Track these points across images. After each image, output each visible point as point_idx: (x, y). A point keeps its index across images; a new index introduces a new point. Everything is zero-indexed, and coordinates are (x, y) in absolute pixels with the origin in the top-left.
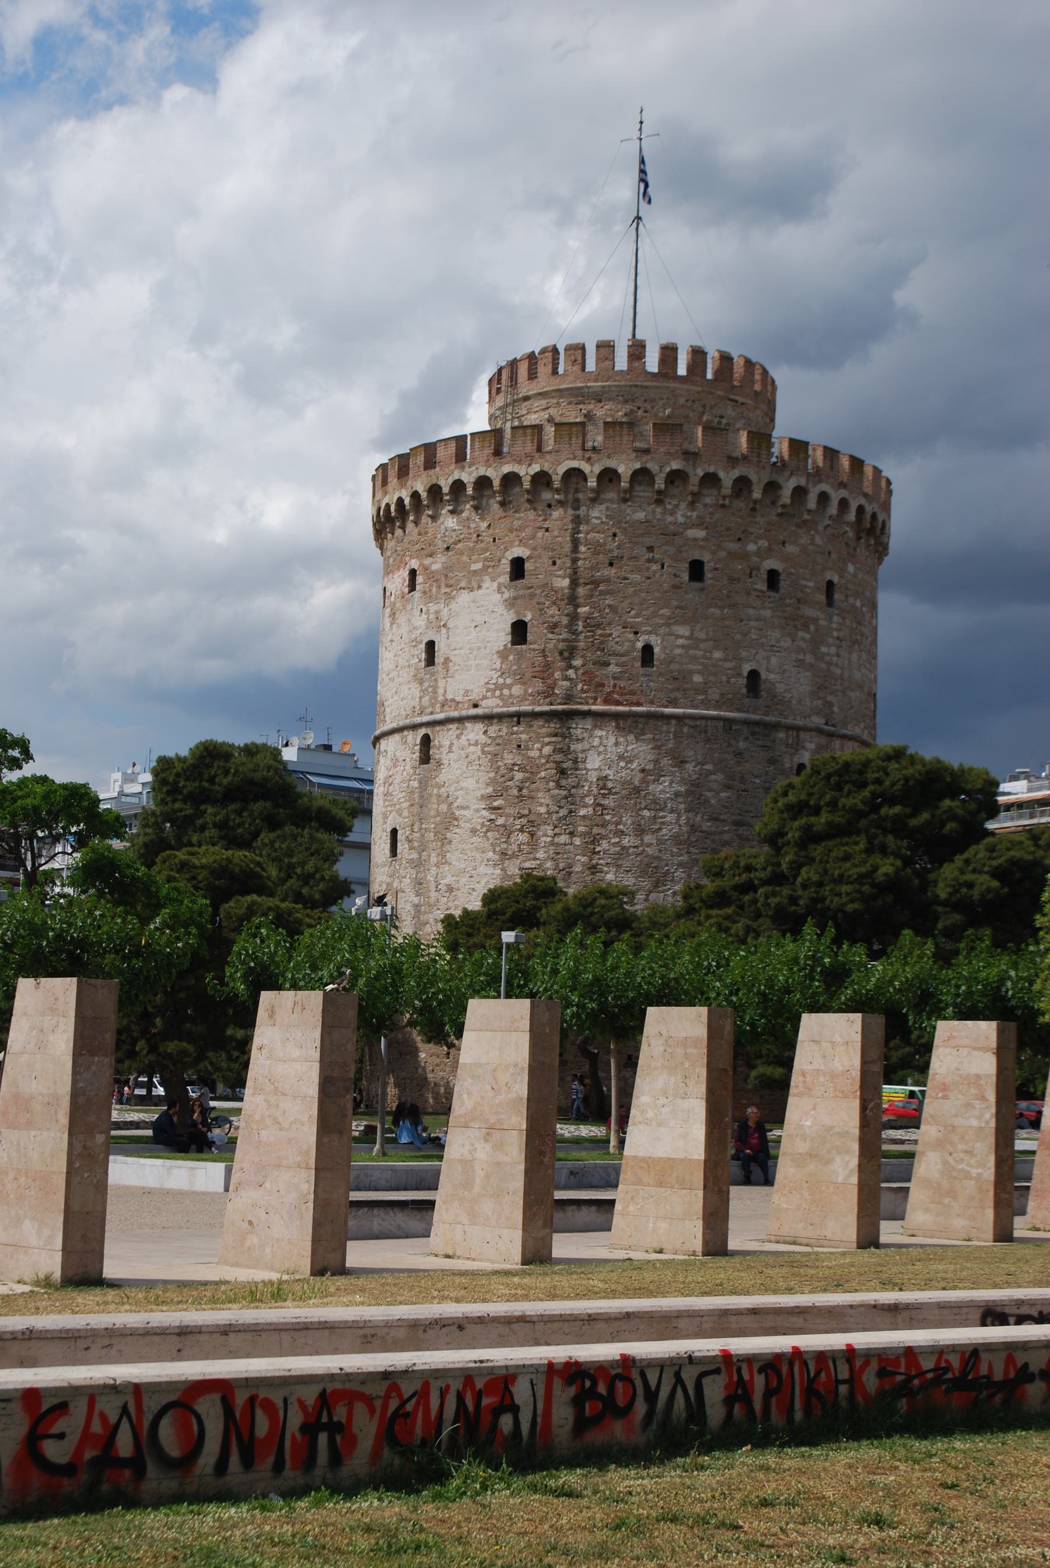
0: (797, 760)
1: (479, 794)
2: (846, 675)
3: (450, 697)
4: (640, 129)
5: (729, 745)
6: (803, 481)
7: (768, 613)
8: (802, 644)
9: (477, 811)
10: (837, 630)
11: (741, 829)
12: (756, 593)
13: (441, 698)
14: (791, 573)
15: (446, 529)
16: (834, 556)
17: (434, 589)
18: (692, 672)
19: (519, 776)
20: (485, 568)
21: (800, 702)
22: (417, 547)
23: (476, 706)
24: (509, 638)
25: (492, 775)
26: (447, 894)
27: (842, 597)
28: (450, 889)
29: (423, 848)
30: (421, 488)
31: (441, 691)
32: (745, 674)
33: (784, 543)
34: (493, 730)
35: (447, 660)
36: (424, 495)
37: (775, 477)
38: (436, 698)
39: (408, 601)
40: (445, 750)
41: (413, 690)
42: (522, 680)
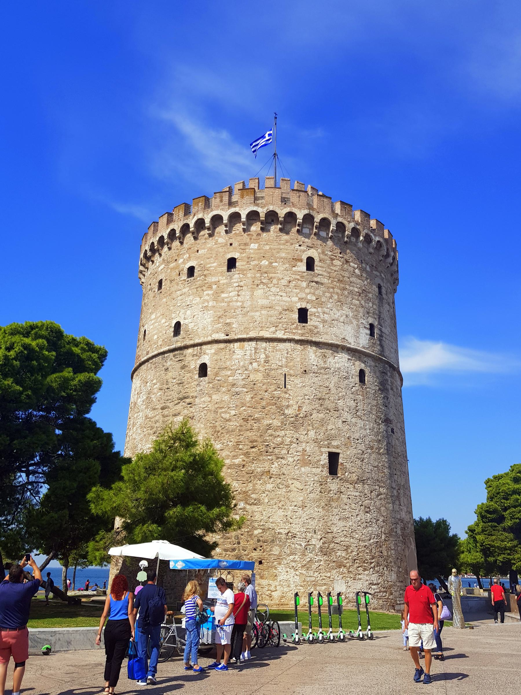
0: (199, 362)
2: (248, 304)
5: (163, 366)
6: (200, 216)
7: (188, 289)
8: (207, 298)
10: (236, 282)
11: (164, 411)
12: (181, 282)
14: (201, 264)
16: (235, 244)
18: (154, 335)
21: (204, 329)
27: (245, 263)
32: (173, 326)
33: (198, 251)
37: (185, 222)
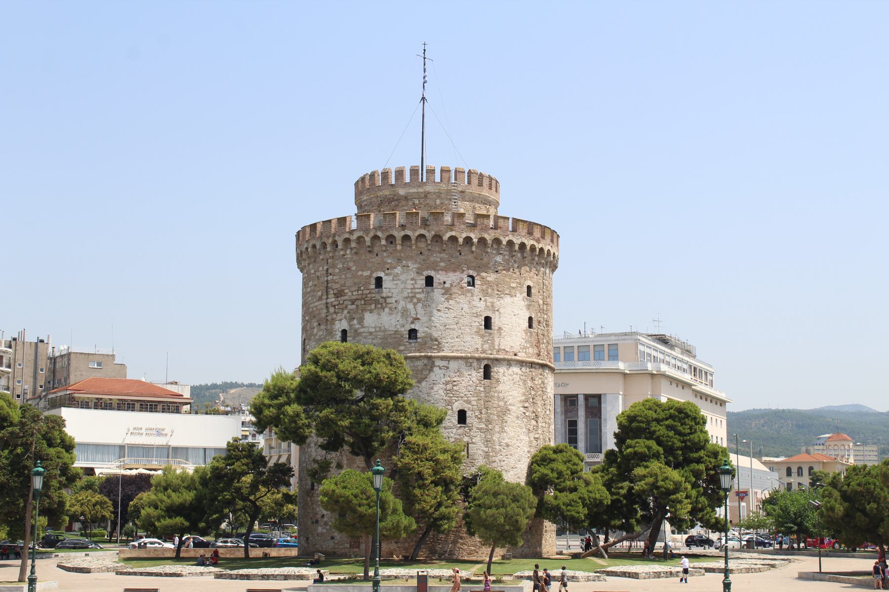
1: (519, 399)
3: (503, 348)
4: (424, 53)
9: (519, 407)
13: (497, 347)
15: (496, 262)
17: (490, 290)
19: (533, 393)
20: (517, 287)
22: (474, 264)
23: (515, 355)
24: (527, 324)
25: (524, 391)
26: (506, 448)
28: (508, 446)
29: (489, 421)
30: (486, 236)
31: (497, 343)
34: (523, 369)
35: (500, 328)
36: (490, 242)
38: (494, 347)
39: (469, 291)
40: (501, 375)
41: (476, 340)
42: (532, 346)
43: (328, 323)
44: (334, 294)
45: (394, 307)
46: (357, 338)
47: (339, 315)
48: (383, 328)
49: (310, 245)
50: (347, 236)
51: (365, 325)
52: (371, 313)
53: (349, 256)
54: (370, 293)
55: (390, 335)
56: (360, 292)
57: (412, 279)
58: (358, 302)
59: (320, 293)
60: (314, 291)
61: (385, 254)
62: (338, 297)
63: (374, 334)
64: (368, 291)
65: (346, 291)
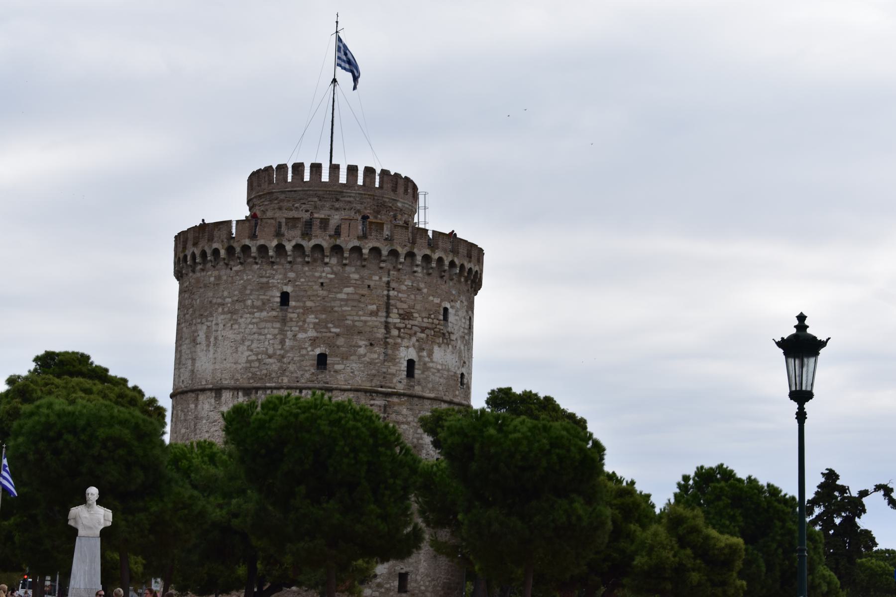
43: (389, 346)
44: (398, 314)
45: (455, 345)
46: (426, 373)
47: (405, 340)
48: (447, 367)
49: (371, 245)
50: (428, 252)
51: (435, 360)
52: (439, 347)
53: (420, 275)
54: (439, 324)
55: (452, 376)
56: (430, 320)
57: (465, 318)
58: (427, 331)
59: (374, 307)
60: (360, 302)
61: (451, 284)
62: (404, 319)
63: (441, 371)
64: (437, 322)
65: (416, 315)
